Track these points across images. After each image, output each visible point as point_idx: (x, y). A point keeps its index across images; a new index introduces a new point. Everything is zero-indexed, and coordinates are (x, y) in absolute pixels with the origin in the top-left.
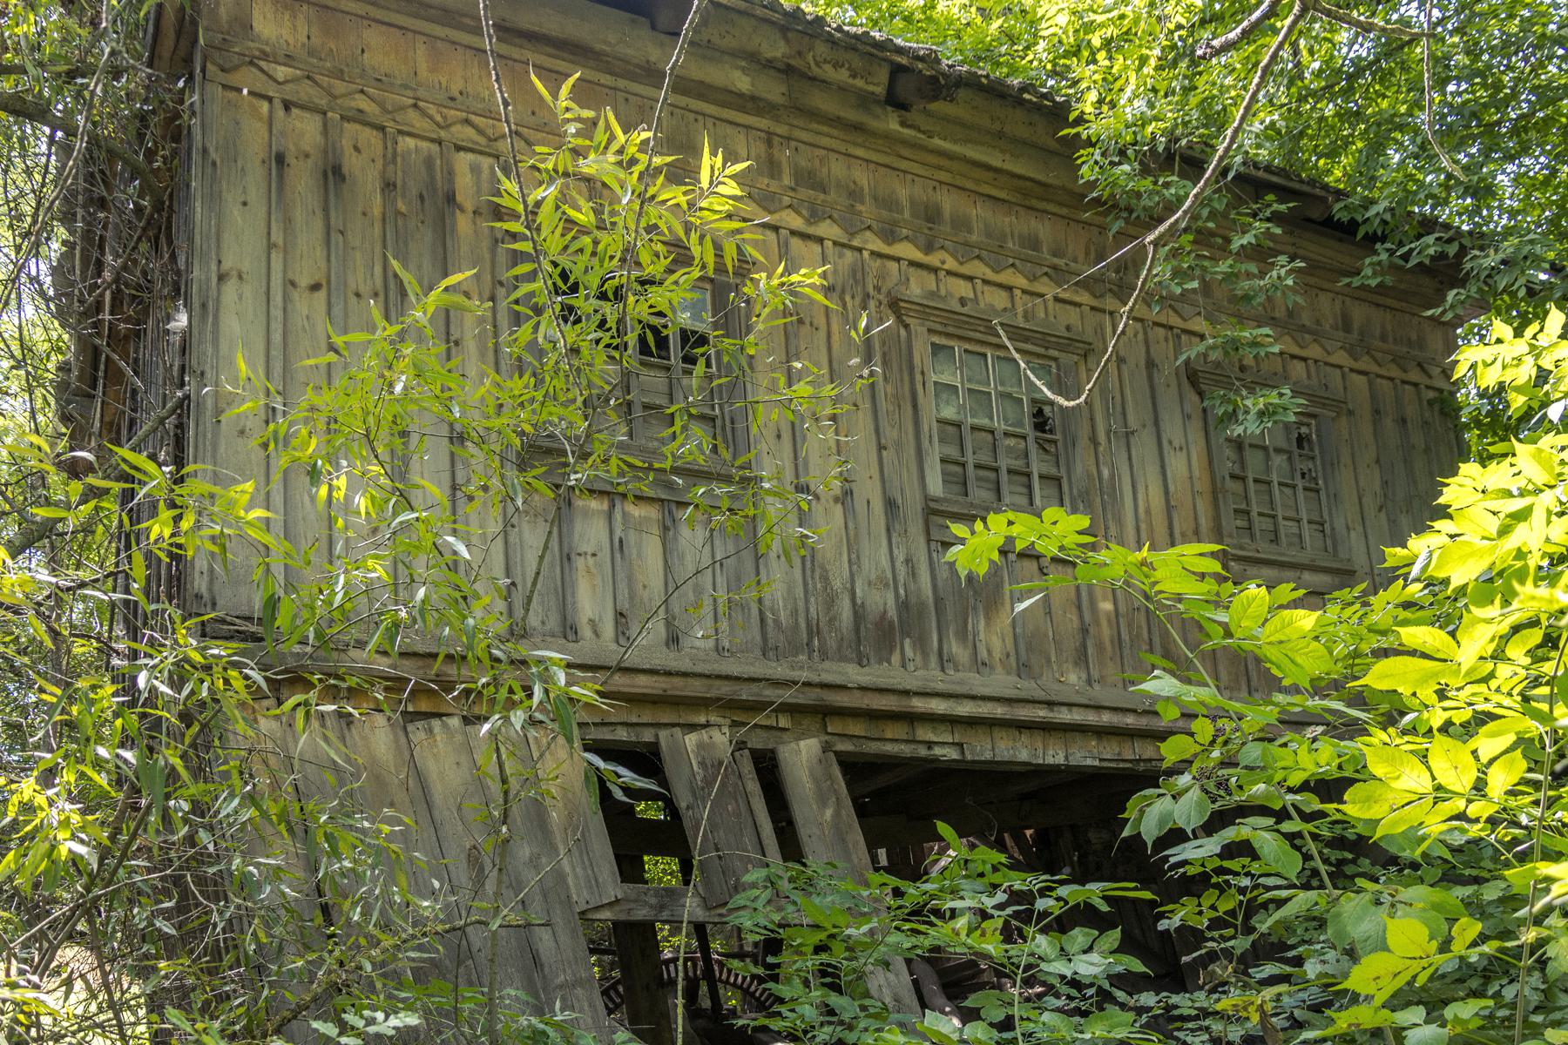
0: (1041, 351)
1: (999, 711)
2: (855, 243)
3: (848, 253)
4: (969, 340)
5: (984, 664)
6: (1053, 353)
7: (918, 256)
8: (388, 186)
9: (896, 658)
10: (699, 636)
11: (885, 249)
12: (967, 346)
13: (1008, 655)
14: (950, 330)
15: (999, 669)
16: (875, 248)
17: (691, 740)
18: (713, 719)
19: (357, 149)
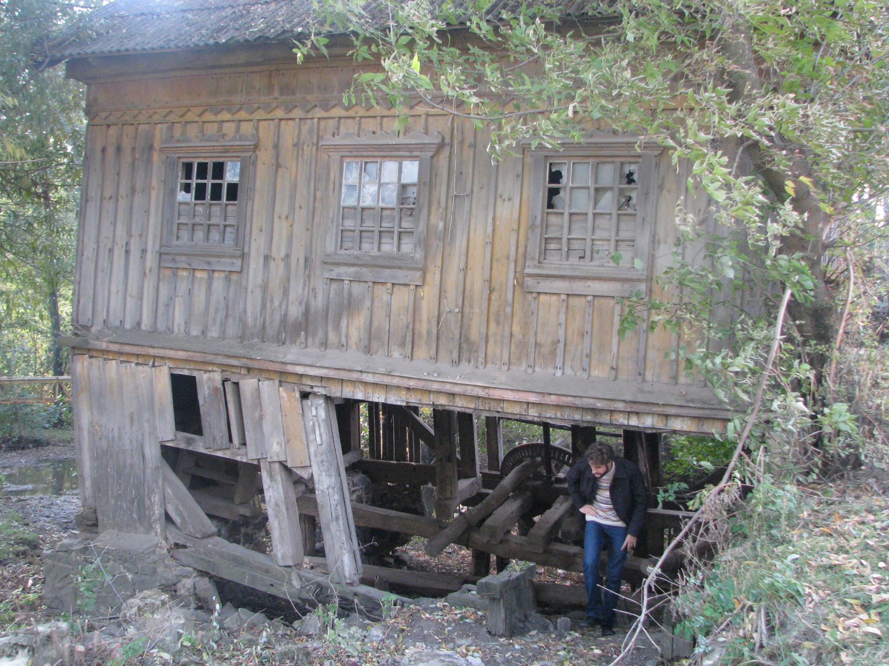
0: (408, 154)
1: (331, 374)
2: (309, 116)
3: (309, 121)
4: (368, 157)
5: (343, 346)
6: (415, 154)
7: (344, 113)
8: (134, 149)
9: (298, 343)
10: (214, 333)
11: (326, 115)
12: (367, 160)
13: (360, 340)
14: (355, 154)
15: (354, 347)
16: (319, 116)
17: (205, 376)
18: (215, 369)
19: (127, 136)
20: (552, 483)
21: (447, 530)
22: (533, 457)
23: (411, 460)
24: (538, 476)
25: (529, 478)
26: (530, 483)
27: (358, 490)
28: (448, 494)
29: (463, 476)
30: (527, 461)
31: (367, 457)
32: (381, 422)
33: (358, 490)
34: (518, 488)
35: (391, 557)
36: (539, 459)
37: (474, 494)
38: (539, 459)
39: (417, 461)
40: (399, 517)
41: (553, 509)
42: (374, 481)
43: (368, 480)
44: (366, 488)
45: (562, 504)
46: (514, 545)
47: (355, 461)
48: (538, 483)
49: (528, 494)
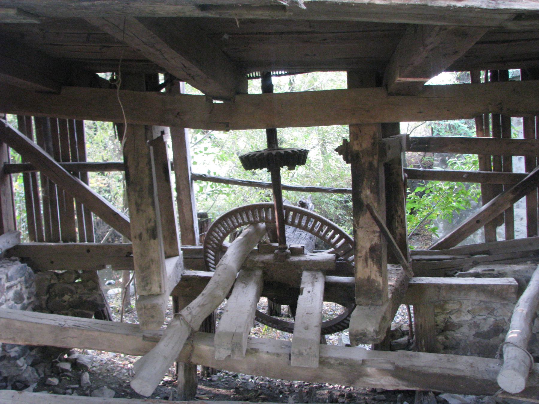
20: (287, 256)
21: (161, 345)
22: (254, 224)
23: (82, 240)
24: (271, 250)
25: (254, 252)
26: (259, 258)
27: (16, 285)
28: (155, 289)
29: (168, 257)
30: (246, 230)
31: (26, 241)
32: (41, 195)
33: (16, 285)
34: (246, 268)
35: (67, 360)
36: (263, 225)
37: (179, 280)
38: (263, 225)
39: (90, 240)
40: (77, 327)
41: (305, 292)
42: (36, 271)
43: (29, 269)
44: (26, 281)
45: (313, 284)
46: (265, 356)
47: (10, 246)
48: (268, 257)
49: (259, 273)
